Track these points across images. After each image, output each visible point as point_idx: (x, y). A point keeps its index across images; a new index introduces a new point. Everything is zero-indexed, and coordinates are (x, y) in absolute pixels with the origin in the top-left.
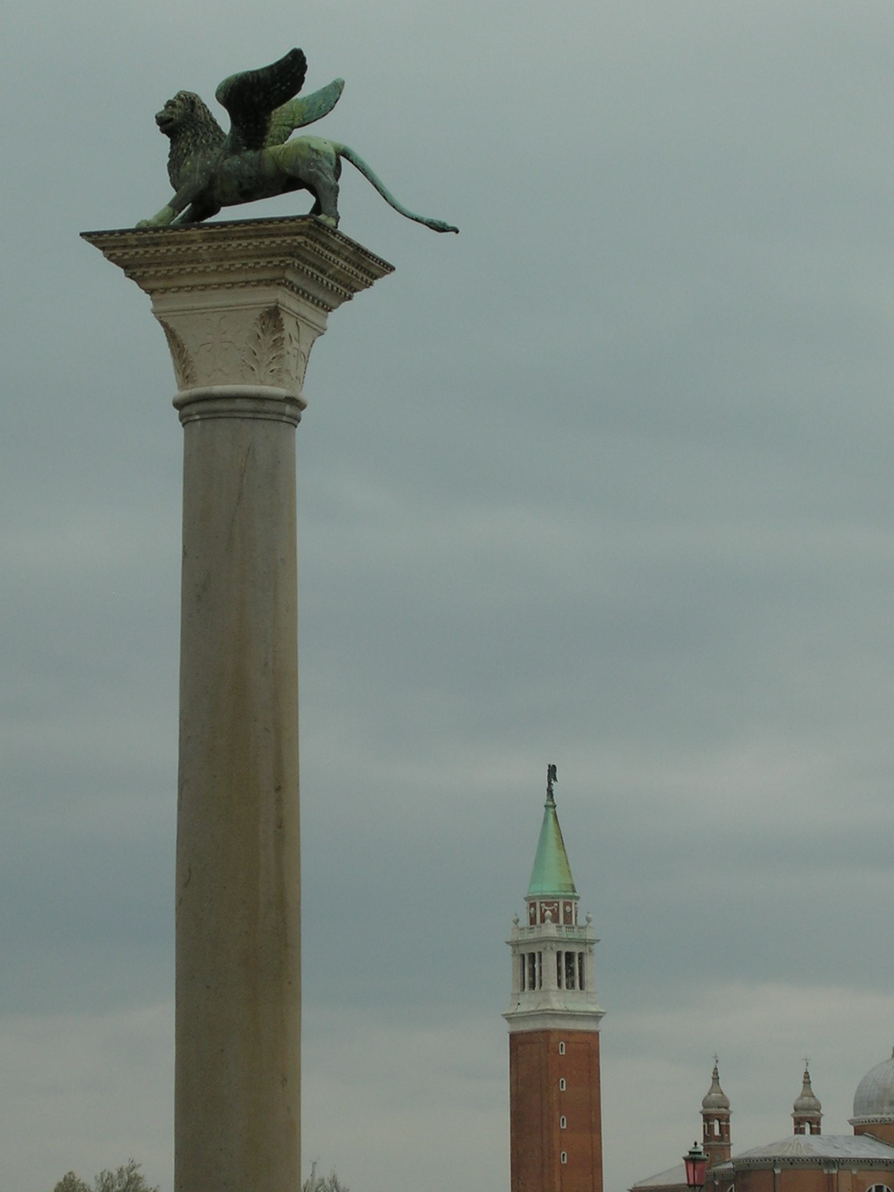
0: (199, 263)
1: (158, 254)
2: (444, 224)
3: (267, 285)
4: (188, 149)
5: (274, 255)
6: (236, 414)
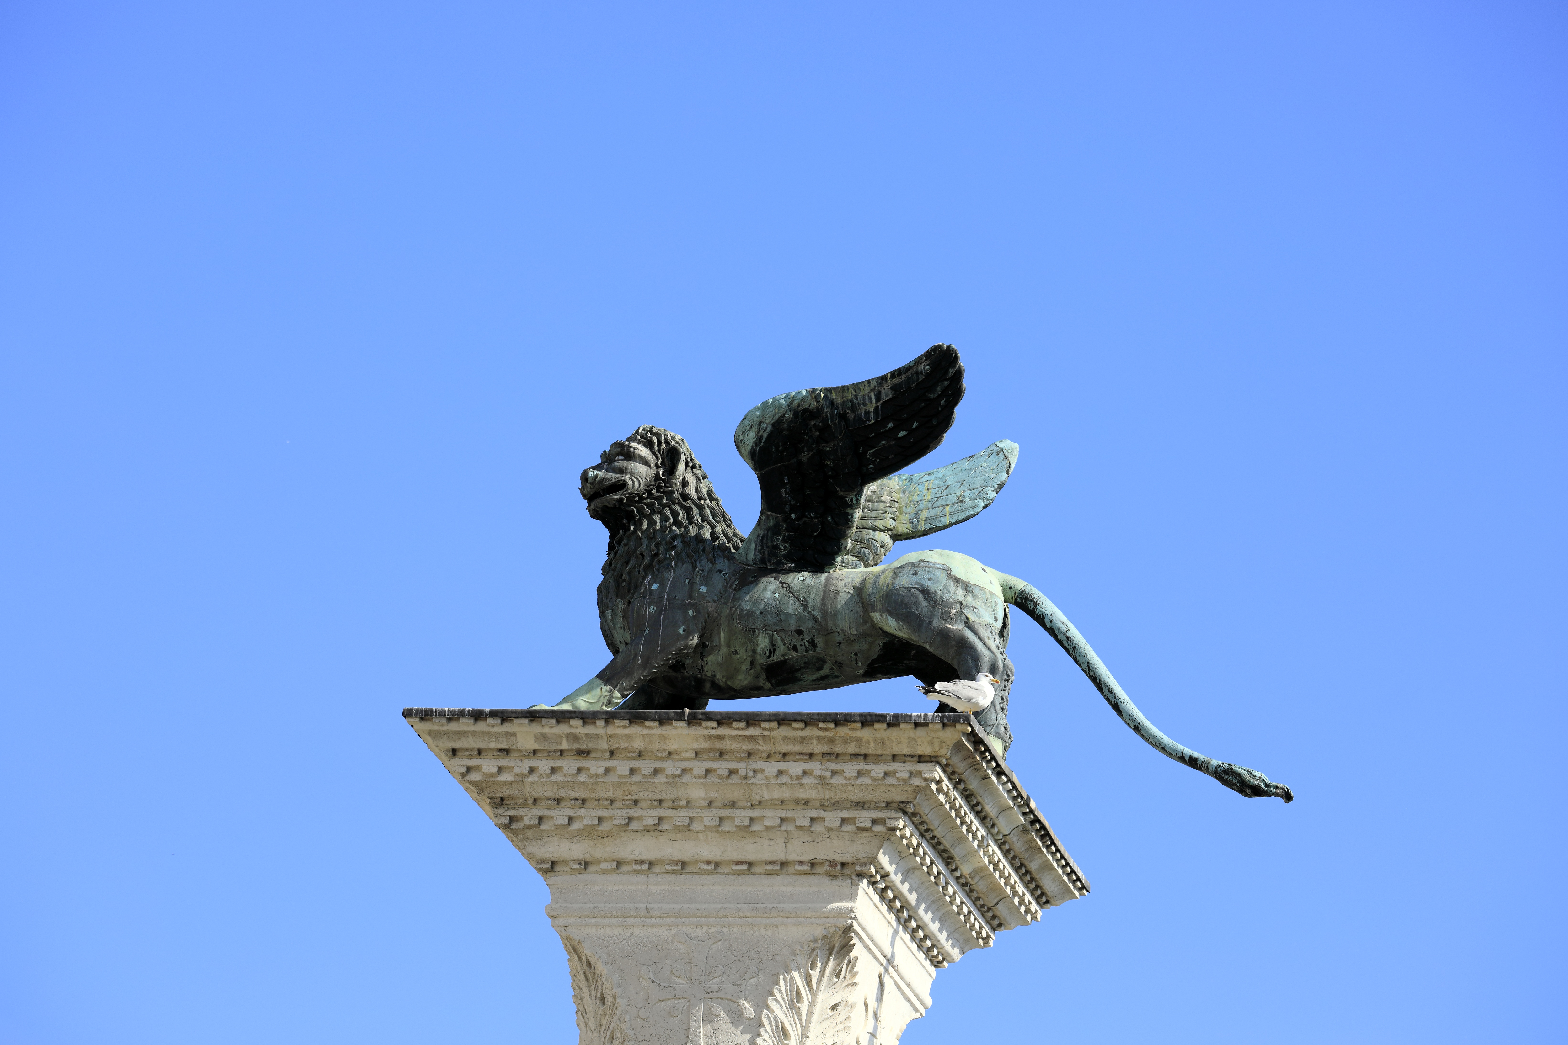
1: (582, 778)
5: (861, 805)
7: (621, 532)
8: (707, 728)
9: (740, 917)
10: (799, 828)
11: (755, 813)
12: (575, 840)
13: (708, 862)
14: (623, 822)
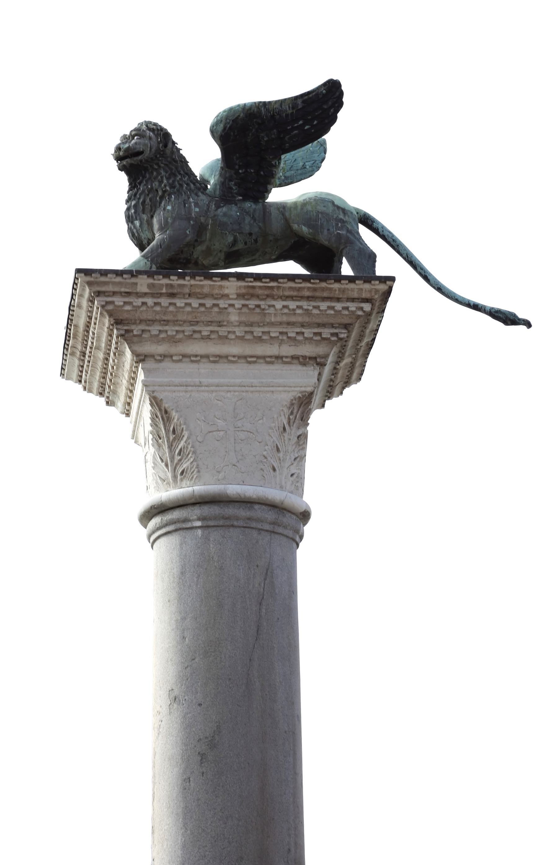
0: (220, 326)
2: (515, 315)
3: (304, 364)
4: (164, 192)
5: (324, 325)
6: (254, 525)
8: (247, 282)
10: (288, 337)
11: (266, 329)
12: (160, 343)
13: (234, 356)
14: (190, 334)
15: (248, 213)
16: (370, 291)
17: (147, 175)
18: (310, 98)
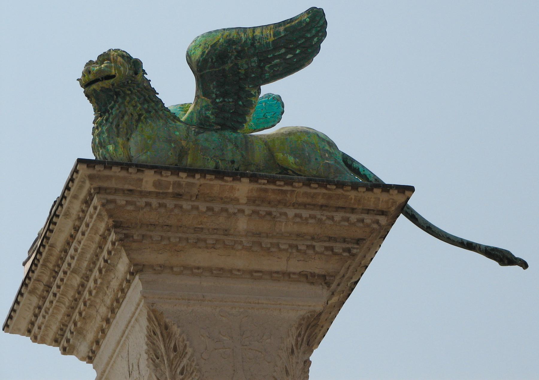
4: (140, 115)
7: (113, 102)
8: (260, 184)
9: (258, 303)
12: (160, 252)
13: (239, 270)
15: (230, 140)
16: (387, 202)
17: (120, 100)
18: (292, 26)
